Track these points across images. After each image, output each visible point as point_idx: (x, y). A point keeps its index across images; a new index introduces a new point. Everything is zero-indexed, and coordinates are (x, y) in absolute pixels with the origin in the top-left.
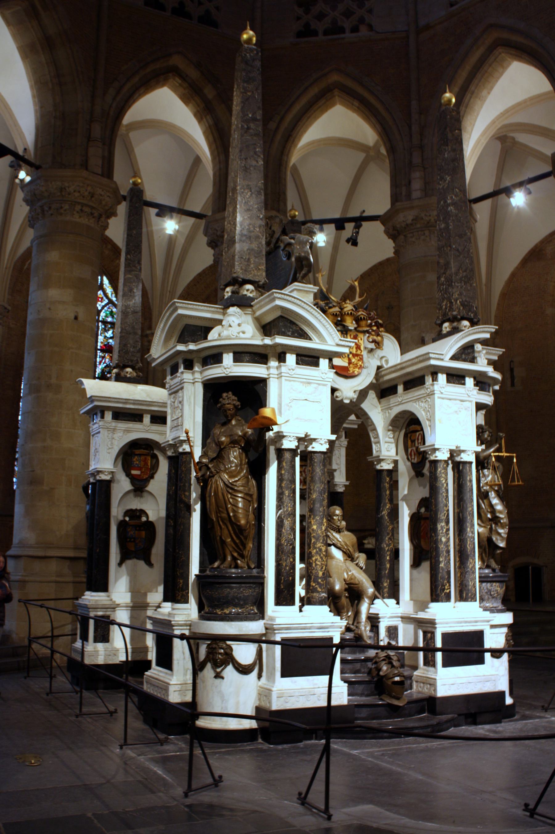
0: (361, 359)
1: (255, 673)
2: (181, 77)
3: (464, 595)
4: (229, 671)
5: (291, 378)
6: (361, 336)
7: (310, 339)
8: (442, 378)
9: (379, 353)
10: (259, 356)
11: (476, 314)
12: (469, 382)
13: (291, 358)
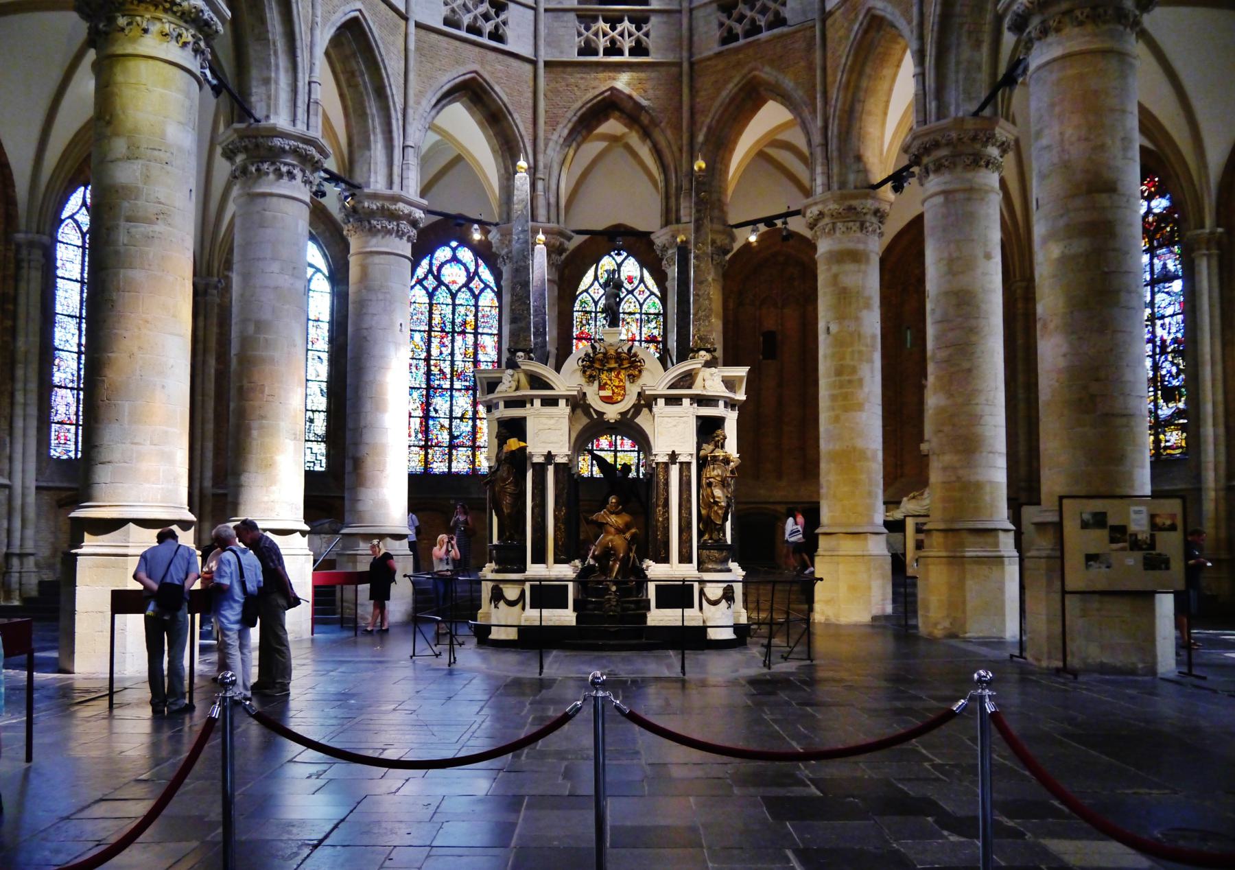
0: (624, 388)
1: (520, 605)
2: (622, 111)
3: (685, 558)
4: (502, 604)
5: (538, 415)
6: (623, 372)
7: (552, 388)
8: (661, 402)
9: (641, 382)
10: (520, 403)
11: (712, 344)
12: (686, 402)
13: (537, 402)
